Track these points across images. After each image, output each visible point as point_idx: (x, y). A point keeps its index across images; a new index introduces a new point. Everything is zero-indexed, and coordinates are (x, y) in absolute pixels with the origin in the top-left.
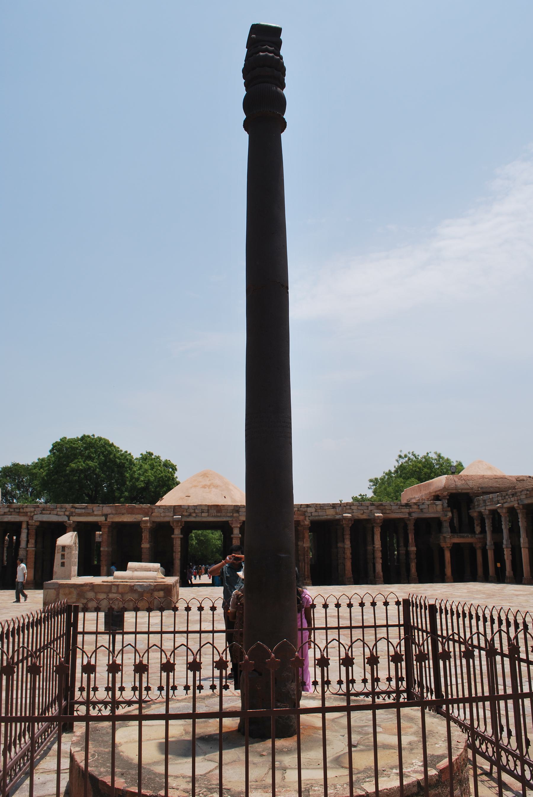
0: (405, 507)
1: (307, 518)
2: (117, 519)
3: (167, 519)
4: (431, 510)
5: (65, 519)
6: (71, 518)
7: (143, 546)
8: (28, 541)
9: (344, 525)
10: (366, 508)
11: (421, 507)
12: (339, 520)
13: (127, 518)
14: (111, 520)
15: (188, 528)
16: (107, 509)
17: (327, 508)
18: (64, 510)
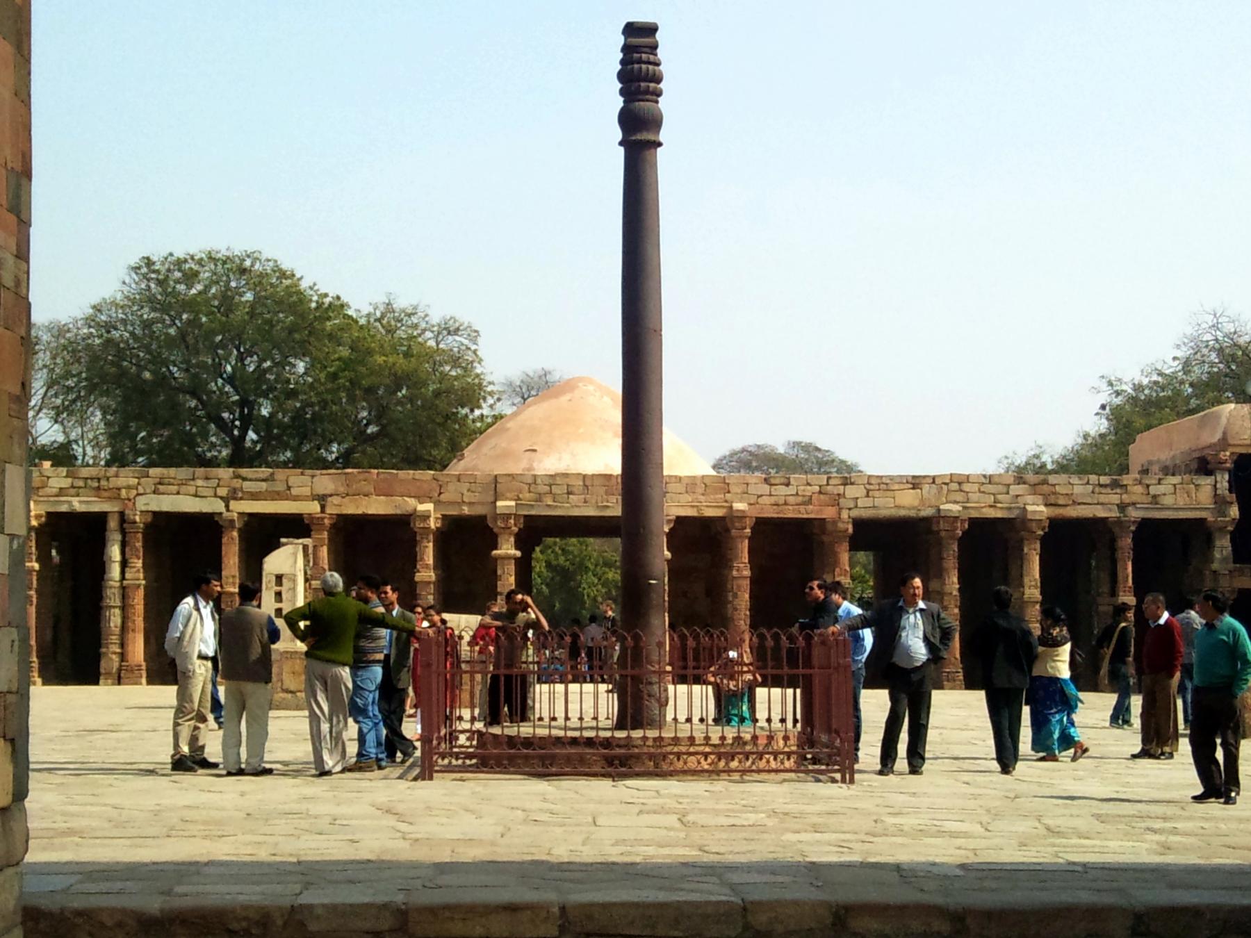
0: (1109, 490)
1: (845, 515)
2: (351, 508)
3: (479, 510)
4: (1182, 501)
5: (217, 506)
6: (233, 504)
7: (419, 577)
8: (124, 564)
9: (943, 534)
10: (1001, 488)
11: (1153, 490)
12: (926, 520)
13: (377, 506)
14: (335, 511)
15: (535, 531)
16: (325, 482)
17: (896, 487)
18: (214, 483)
